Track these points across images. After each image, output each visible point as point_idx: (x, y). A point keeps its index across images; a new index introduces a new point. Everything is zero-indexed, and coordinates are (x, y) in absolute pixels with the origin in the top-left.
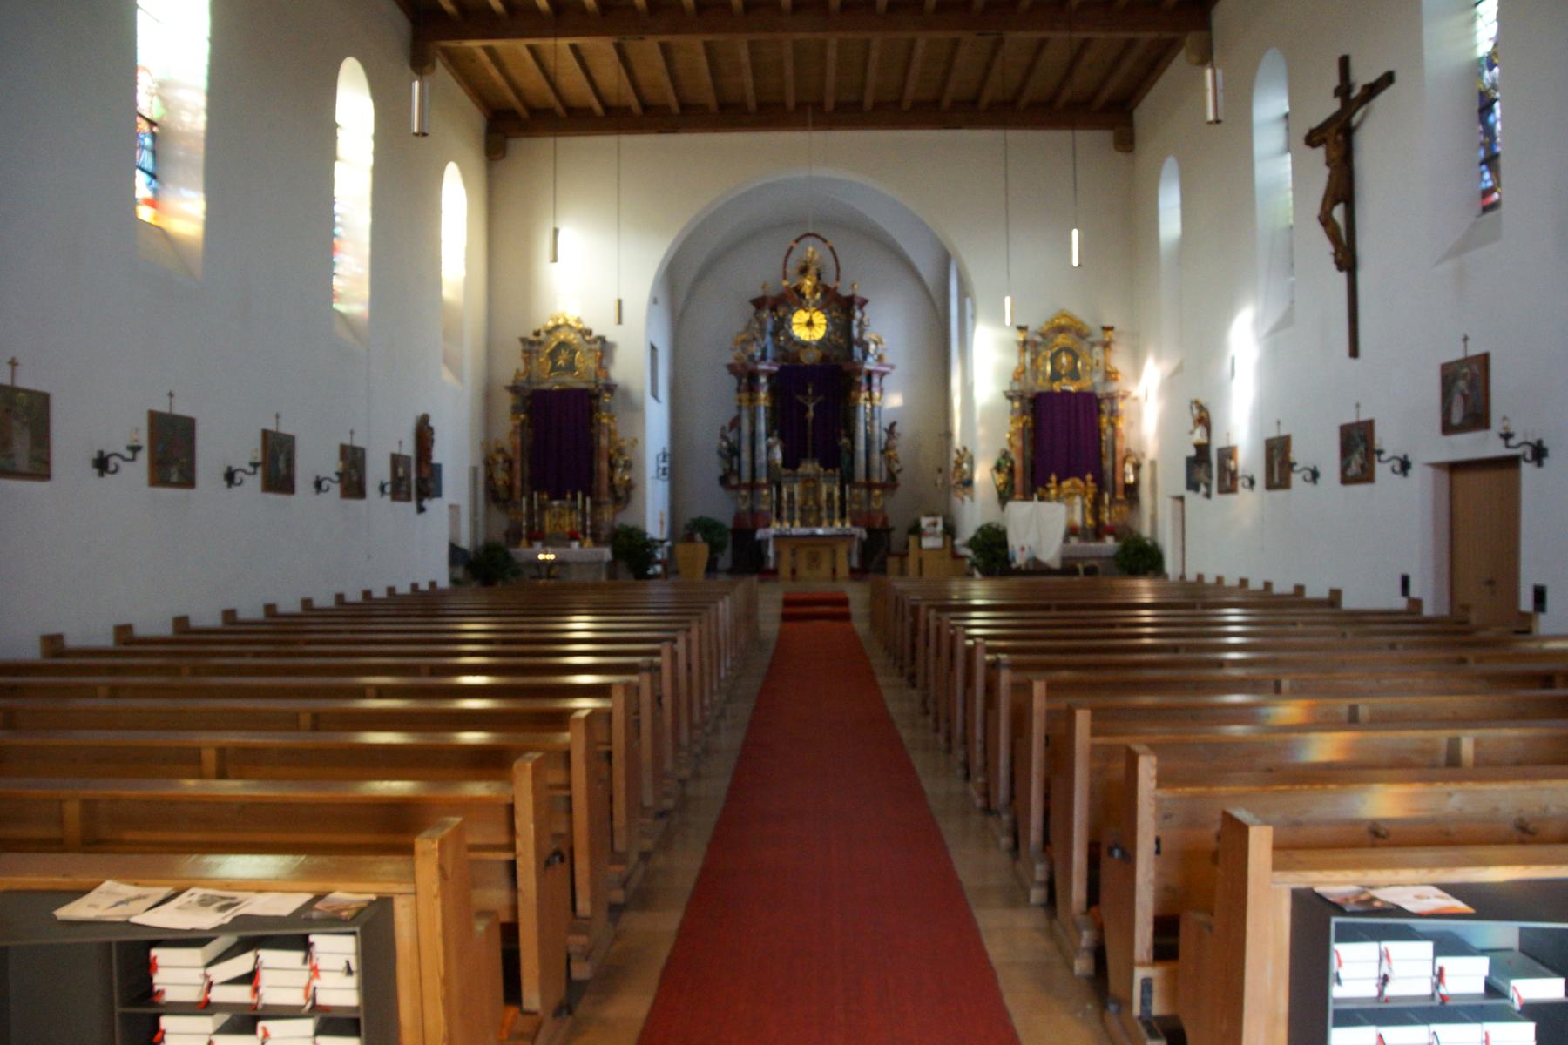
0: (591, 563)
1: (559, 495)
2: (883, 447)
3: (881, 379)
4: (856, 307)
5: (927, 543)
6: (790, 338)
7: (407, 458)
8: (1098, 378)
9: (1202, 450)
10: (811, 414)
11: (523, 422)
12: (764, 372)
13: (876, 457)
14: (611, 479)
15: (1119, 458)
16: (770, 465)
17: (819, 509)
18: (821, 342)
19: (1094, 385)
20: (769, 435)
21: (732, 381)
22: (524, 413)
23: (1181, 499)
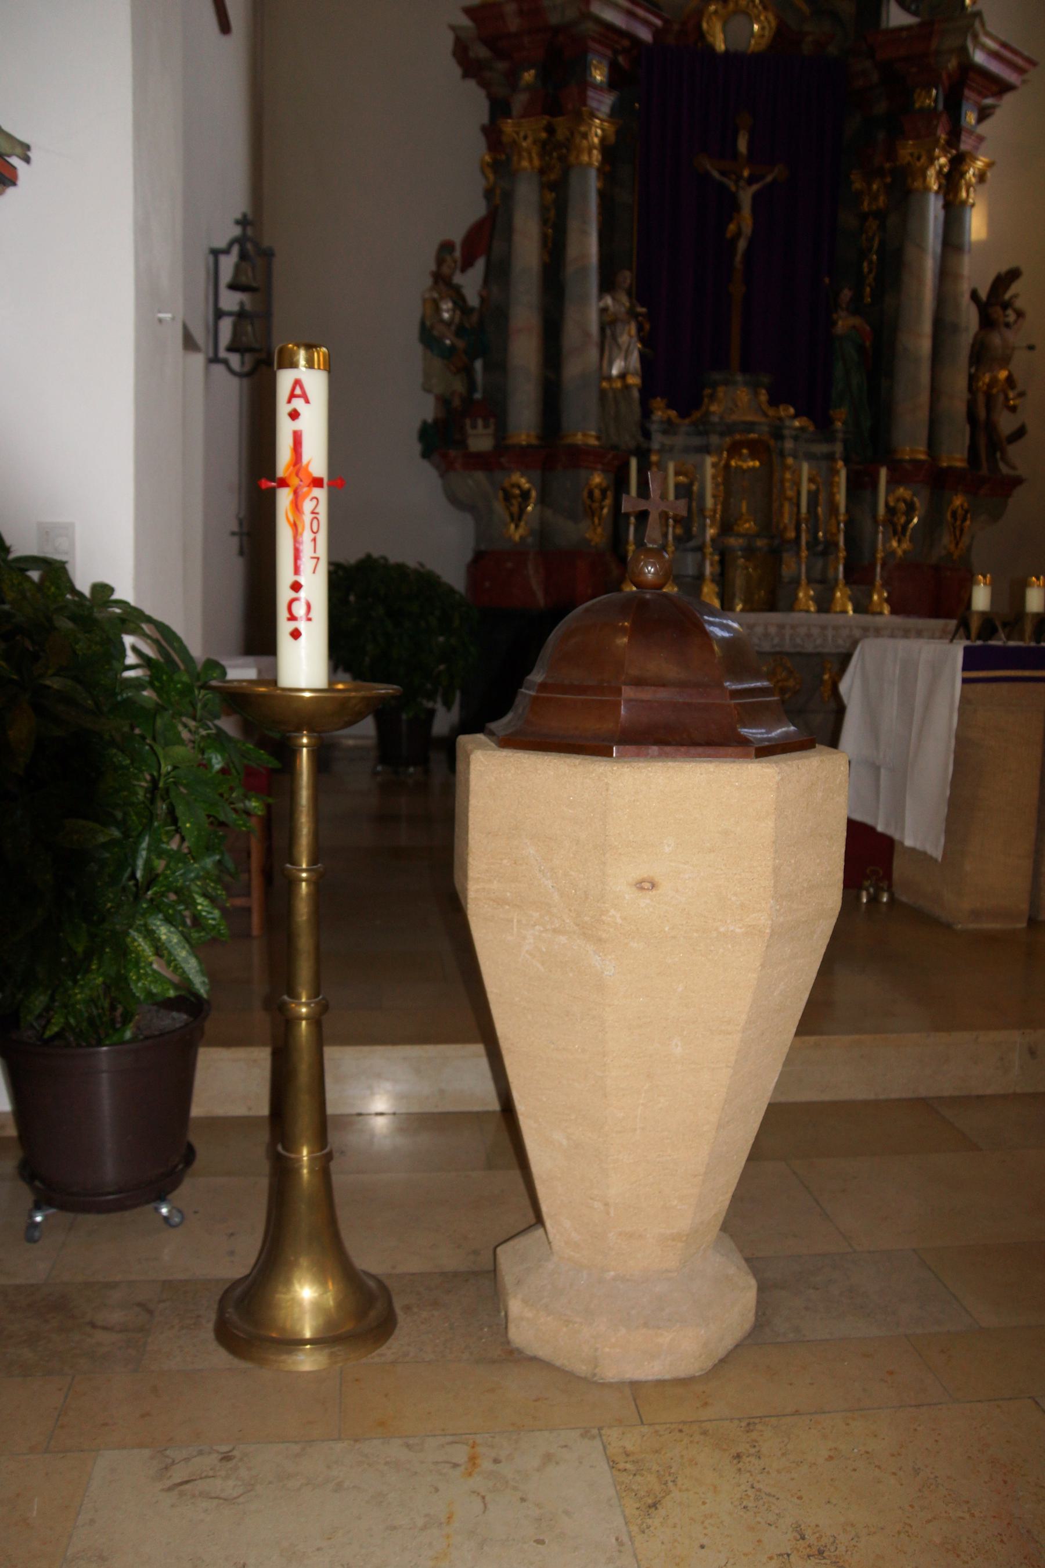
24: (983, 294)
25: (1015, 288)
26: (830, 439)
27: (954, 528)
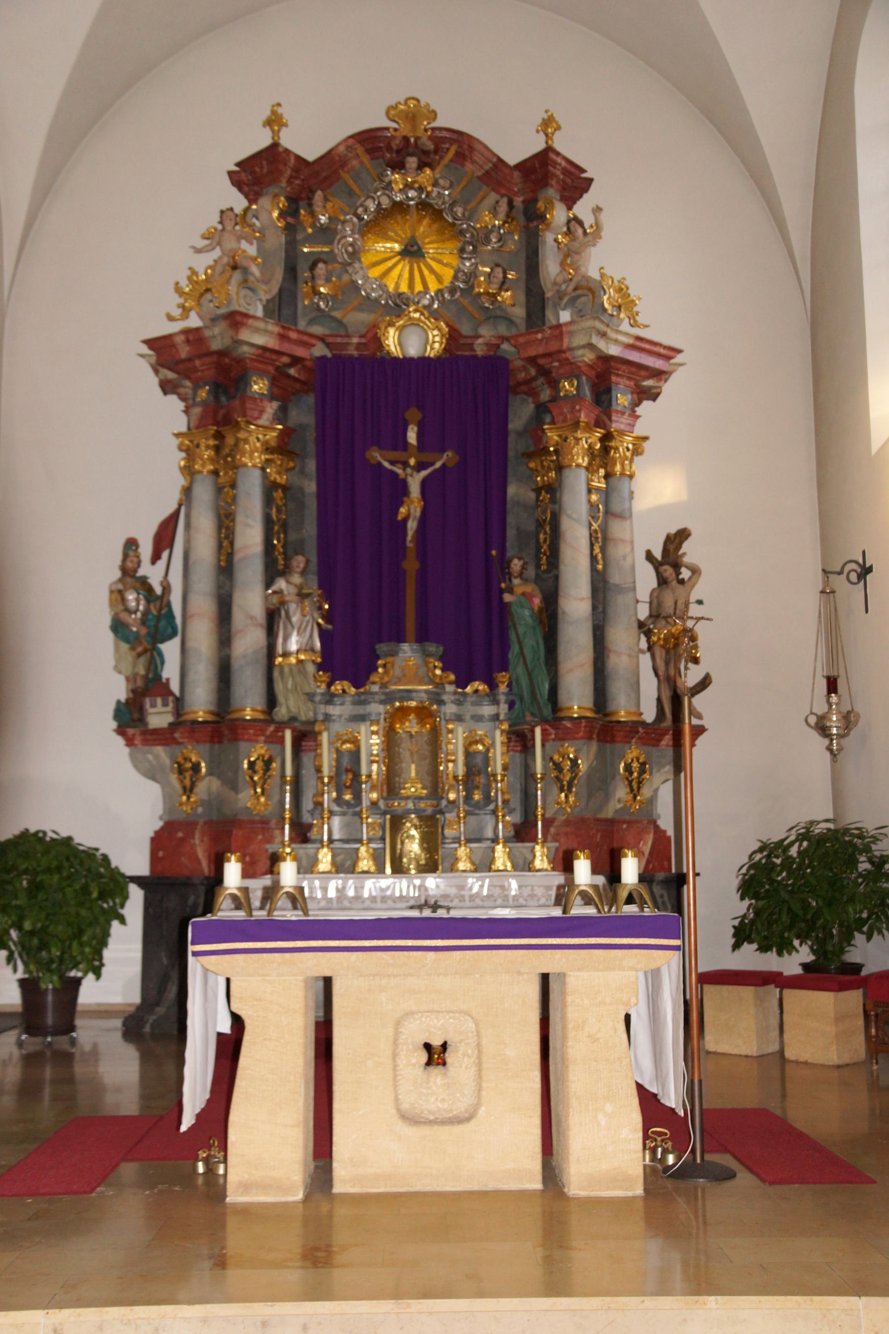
2: (643, 612)
24: (658, 554)
25: (686, 547)
26: (495, 702)
27: (630, 782)
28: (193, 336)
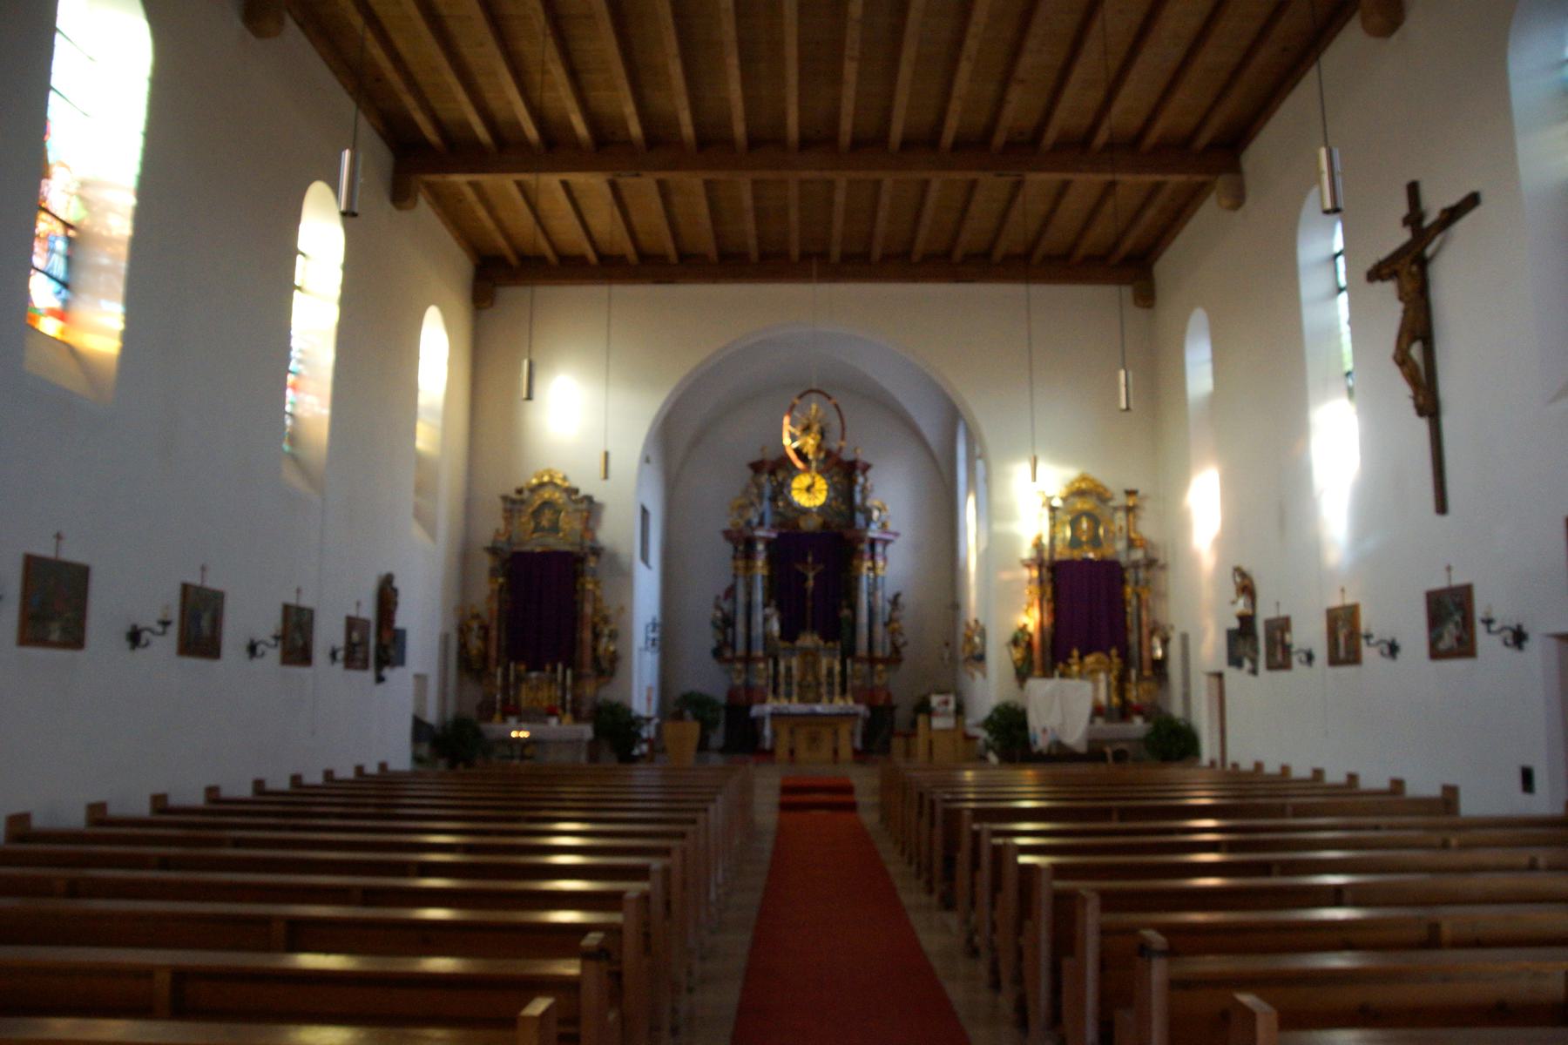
0: (570, 742)
1: (541, 668)
3: (884, 548)
4: (858, 472)
5: (938, 723)
6: (790, 503)
7: (366, 623)
8: (1121, 545)
9: (1247, 621)
10: (810, 583)
11: (501, 586)
12: (762, 538)
13: (879, 630)
14: (595, 649)
15: (1145, 631)
16: (767, 637)
17: (819, 684)
18: (822, 508)
19: (1117, 553)
20: (765, 605)
21: (728, 548)
22: (502, 576)
23: (1220, 676)
28: (740, 531)
